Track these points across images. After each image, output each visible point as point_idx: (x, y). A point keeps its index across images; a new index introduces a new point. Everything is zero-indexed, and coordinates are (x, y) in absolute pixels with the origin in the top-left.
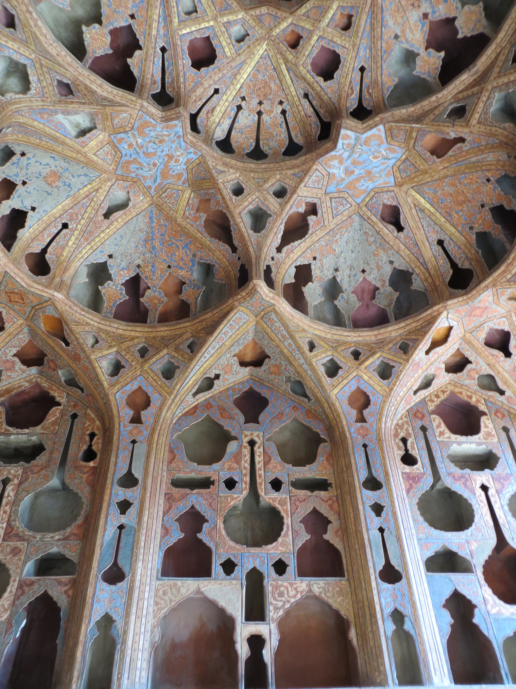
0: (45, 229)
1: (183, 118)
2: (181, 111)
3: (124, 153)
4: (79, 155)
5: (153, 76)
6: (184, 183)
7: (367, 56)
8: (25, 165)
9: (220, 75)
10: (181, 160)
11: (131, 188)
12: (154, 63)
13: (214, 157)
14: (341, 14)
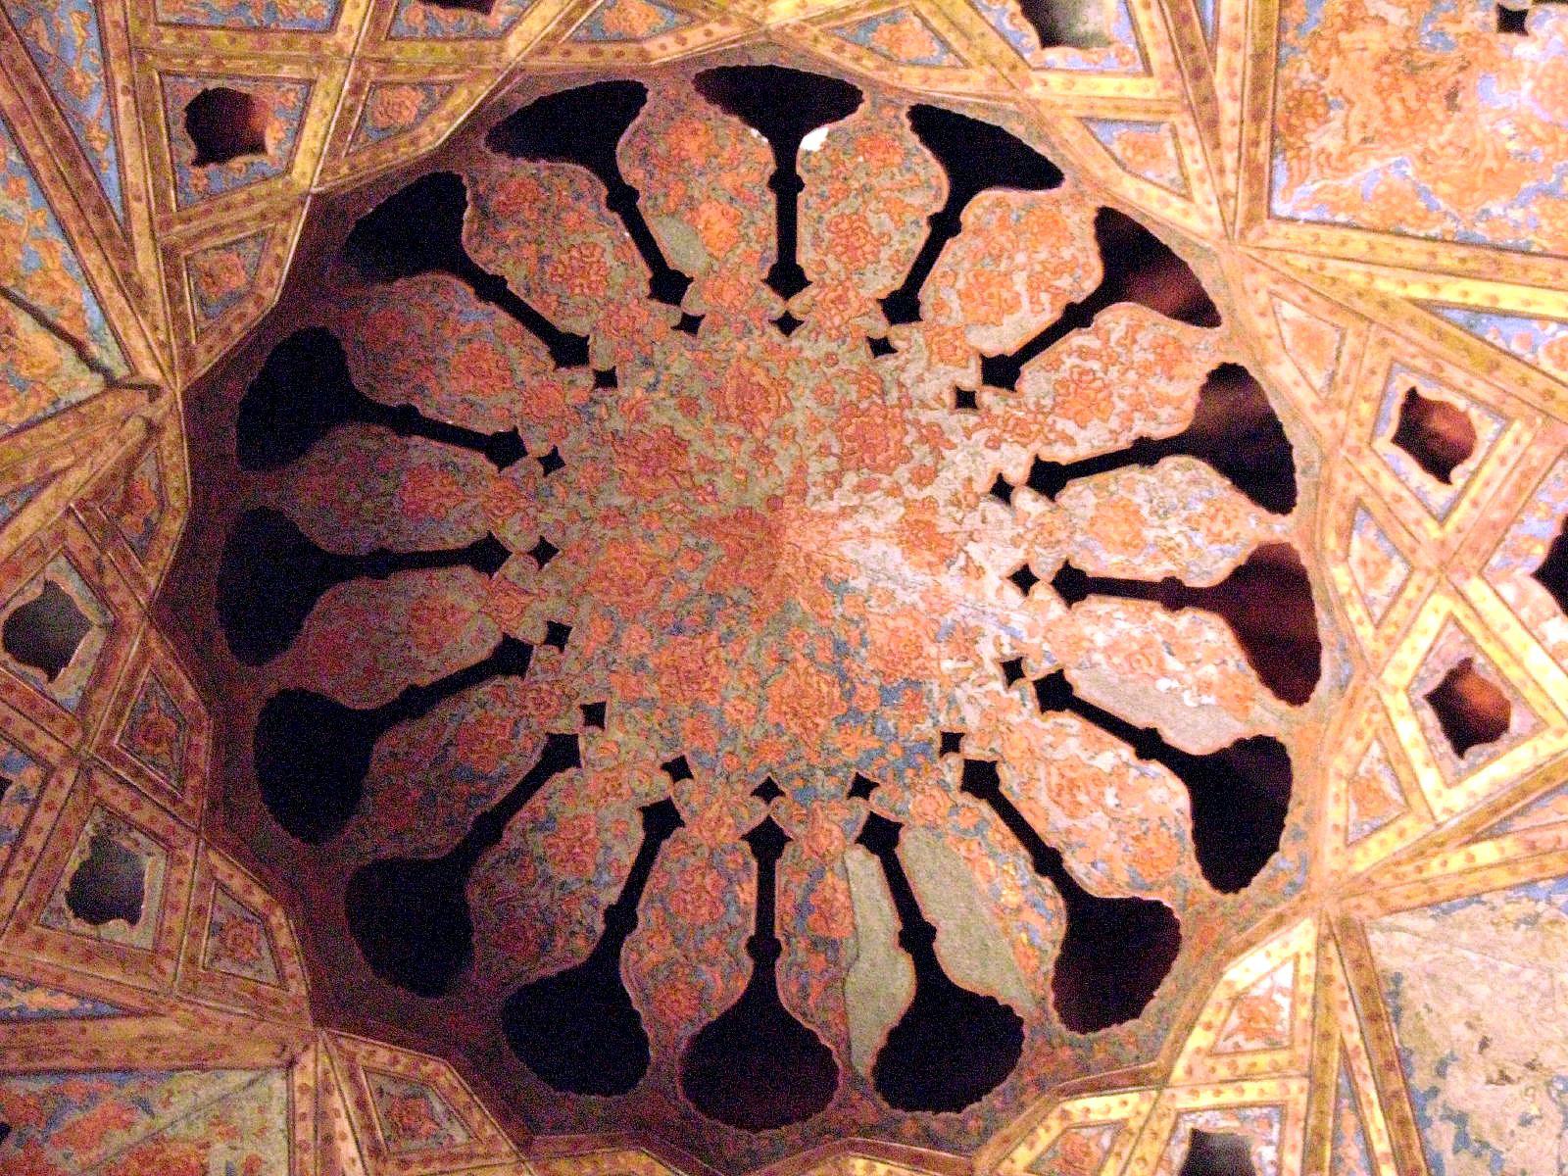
7: (38, 26)
14: (258, 147)
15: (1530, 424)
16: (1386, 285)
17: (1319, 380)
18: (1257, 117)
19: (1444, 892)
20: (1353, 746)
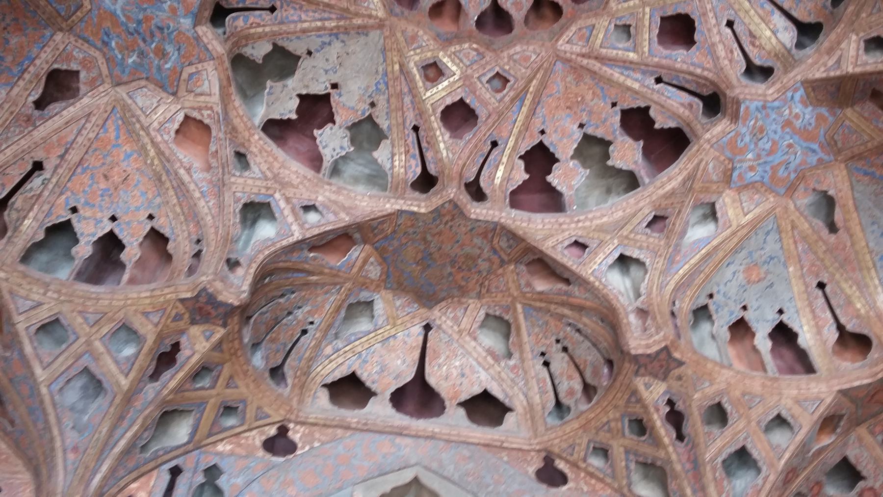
0: (813, 311)
1: (741, 97)
2: (732, 95)
3: (757, 178)
4: (739, 233)
5: (682, 105)
6: (834, 115)
8: (723, 299)
9: (711, 15)
10: (797, 111)
11: (809, 184)
12: (669, 98)
13: (812, 65)
15: (498, 107)
16: (534, 82)
17: (515, 57)
18: (582, 67)
19: (389, 54)
20: (425, 38)
